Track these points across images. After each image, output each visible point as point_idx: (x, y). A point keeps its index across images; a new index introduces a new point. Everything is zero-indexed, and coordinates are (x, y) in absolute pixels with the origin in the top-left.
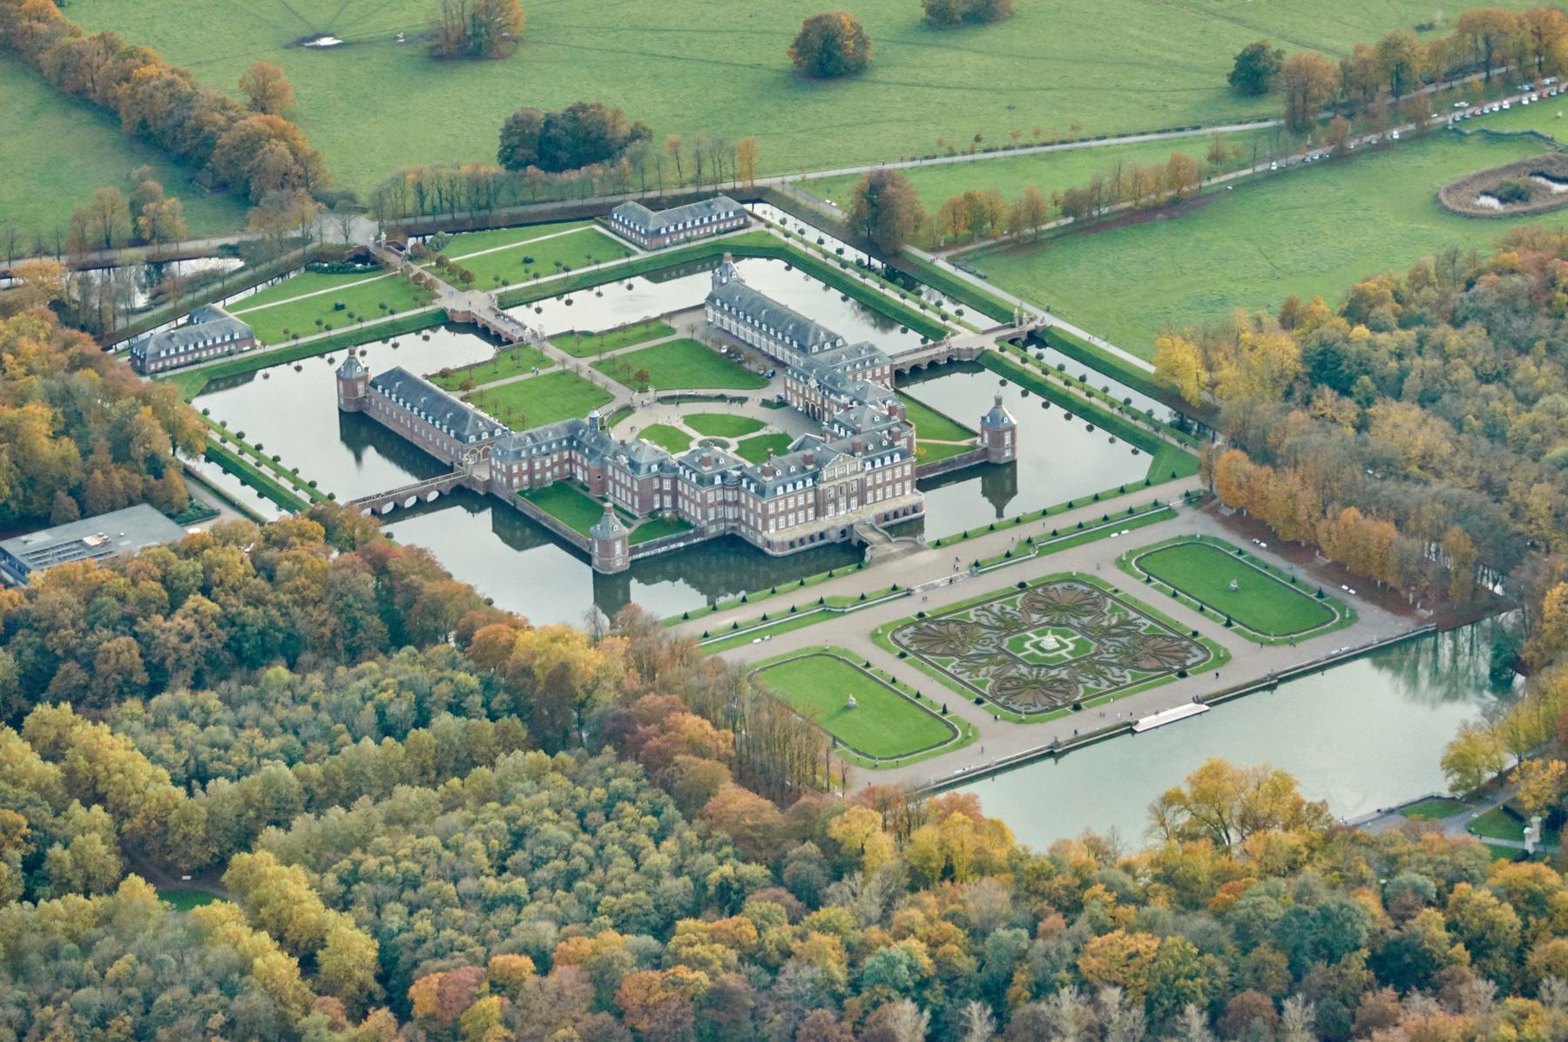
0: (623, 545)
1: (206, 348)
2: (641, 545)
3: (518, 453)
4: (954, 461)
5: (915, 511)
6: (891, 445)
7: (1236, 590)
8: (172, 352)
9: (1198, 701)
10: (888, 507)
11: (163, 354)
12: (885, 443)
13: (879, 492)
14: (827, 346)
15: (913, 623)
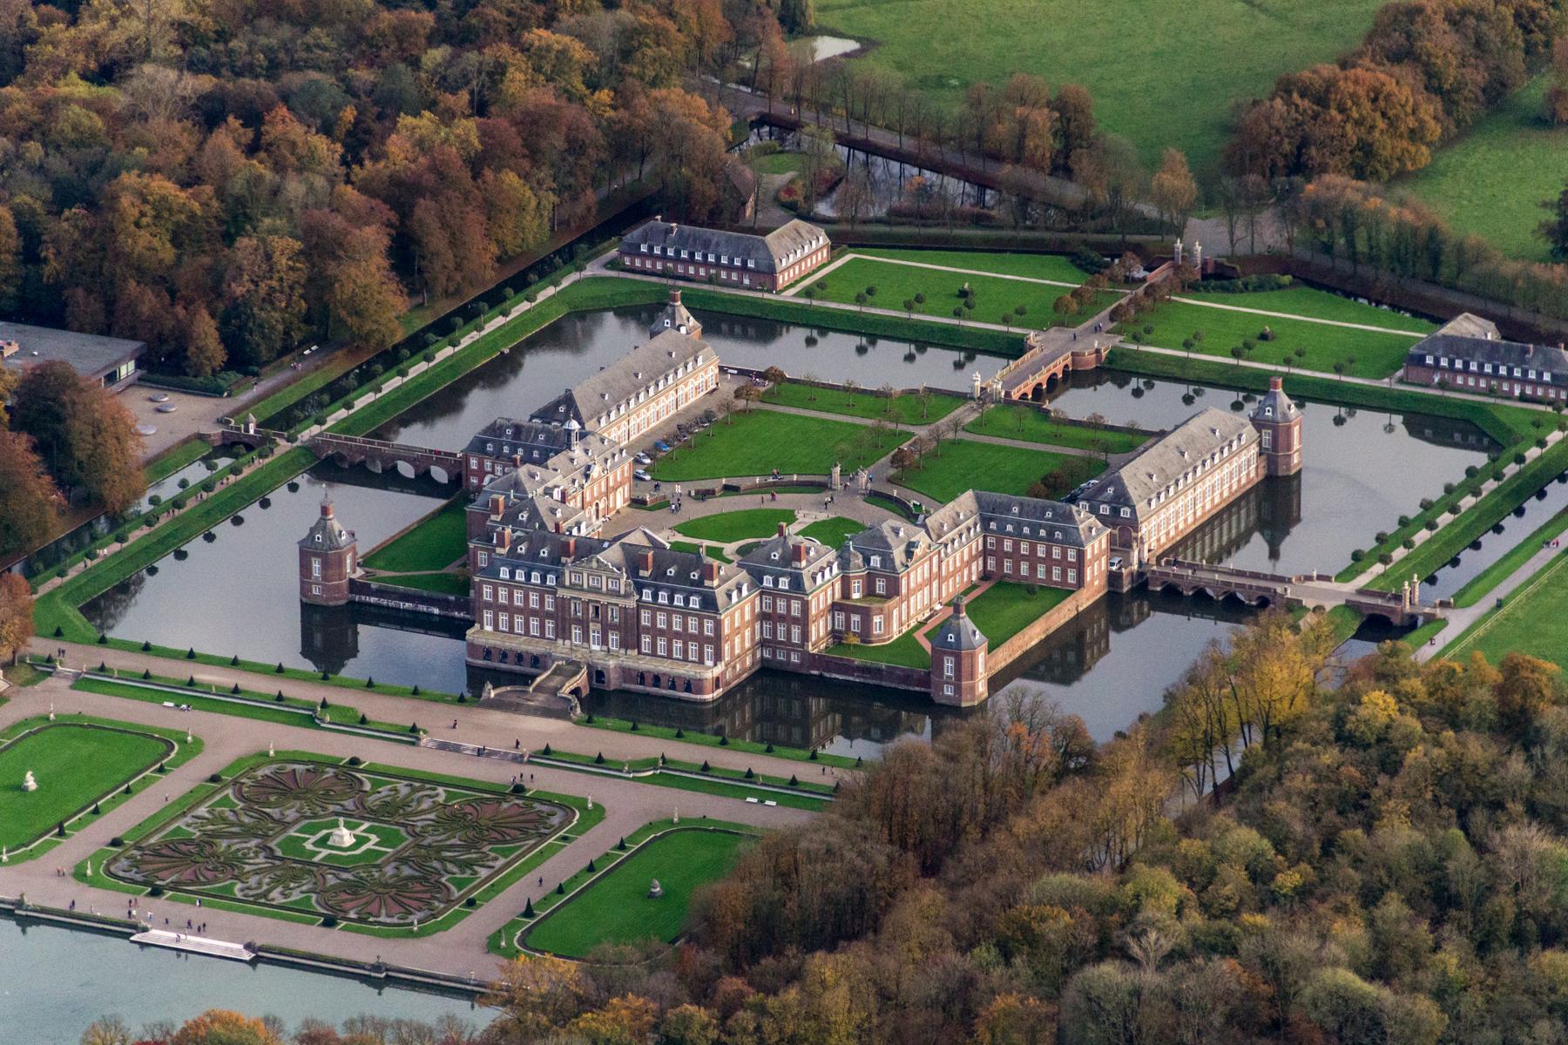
0: (325, 566)
1: (705, 263)
2: (374, 585)
3: (484, 442)
4: (879, 670)
5: (688, 689)
6: (700, 583)
7: (652, 896)
8: (657, 251)
9: (248, 947)
10: (664, 667)
11: (644, 249)
12: (695, 575)
13: (661, 642)
14: (1105, 509)
15: (318, 764)
